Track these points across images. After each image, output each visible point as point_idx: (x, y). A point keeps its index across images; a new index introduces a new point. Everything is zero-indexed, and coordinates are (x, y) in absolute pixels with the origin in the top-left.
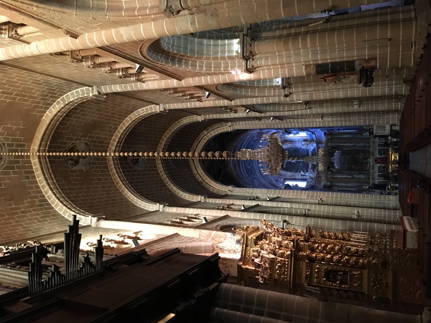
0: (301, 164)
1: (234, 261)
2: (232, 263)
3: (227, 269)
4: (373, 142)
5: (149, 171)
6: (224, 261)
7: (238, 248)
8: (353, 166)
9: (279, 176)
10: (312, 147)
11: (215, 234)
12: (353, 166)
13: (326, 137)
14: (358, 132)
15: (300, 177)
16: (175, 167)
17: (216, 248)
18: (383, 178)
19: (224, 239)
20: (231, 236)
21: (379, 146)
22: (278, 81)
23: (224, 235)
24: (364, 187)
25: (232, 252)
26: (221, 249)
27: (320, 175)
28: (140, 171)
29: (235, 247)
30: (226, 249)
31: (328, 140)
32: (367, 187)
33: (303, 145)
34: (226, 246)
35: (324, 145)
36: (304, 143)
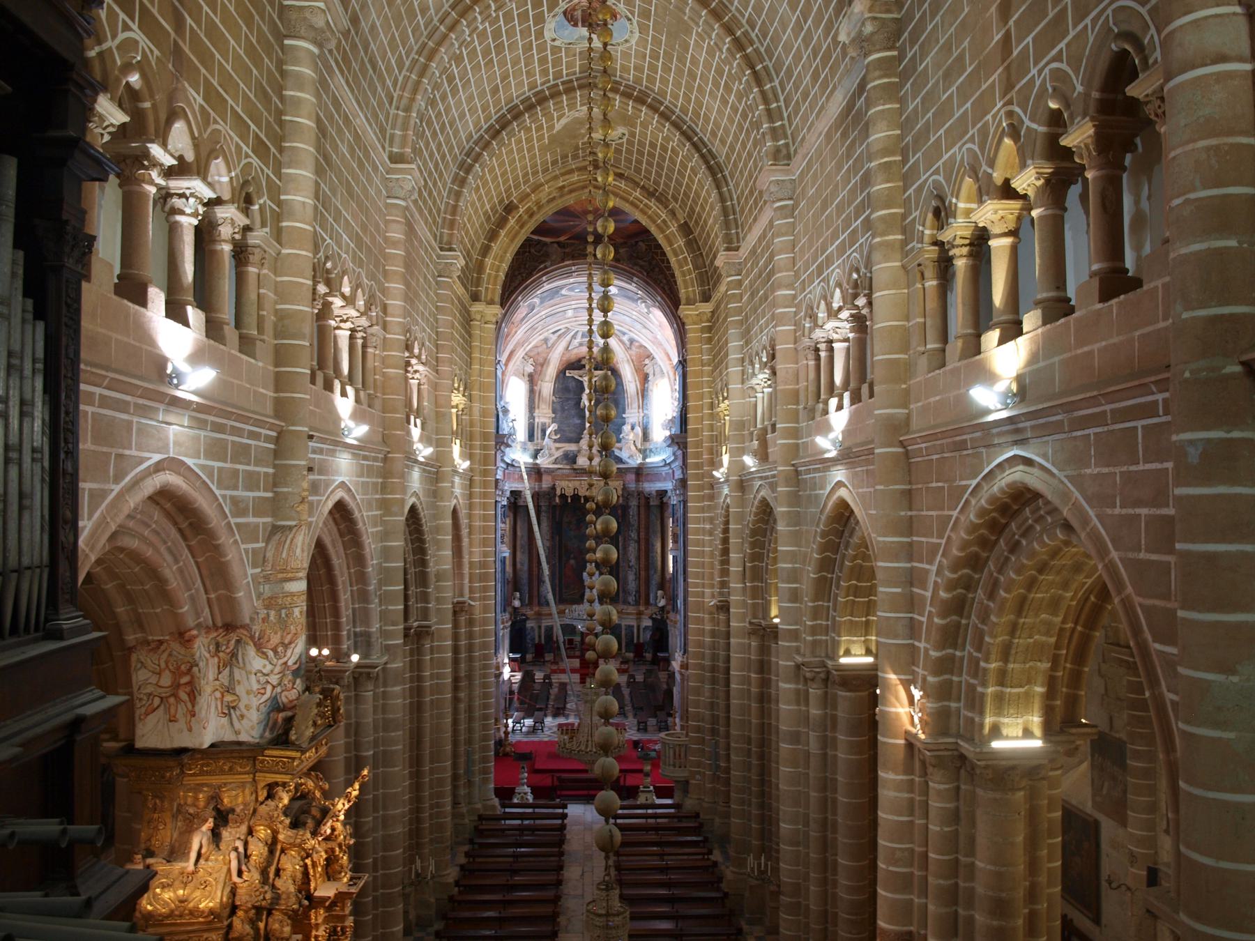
0: (578, 421)
1: (190, 730)
2: (182, 724)
3: (157, 701)
4: (640, 614)
5: (543, 61)
6: (188, 689)
7: (244, 722)
8: (572, 562)
9: (541, 360)
10: (628, 455)
11: (292, 595)
12: (572, 562)
13: (654, 493)
14: (668, 577)
15: (539, 420)
16: (558, 127)
17: (234, 637)
18: (543, 642)
19: (275, 651)
20: (290, 663)
21: (630, 627)
22: (853, 652)
23: (293, 631)
24: (518, 594)
25: (228, 698)
26: (234, 655)
27: (544, 477)
28: (540, 34)
29: (248, 707)
30: (238, 674)
31: (645, 498)
32: (517, 603)
33: (633, 428)
34: (248, 673)
35: (632, 486)
36: (639, 430)
